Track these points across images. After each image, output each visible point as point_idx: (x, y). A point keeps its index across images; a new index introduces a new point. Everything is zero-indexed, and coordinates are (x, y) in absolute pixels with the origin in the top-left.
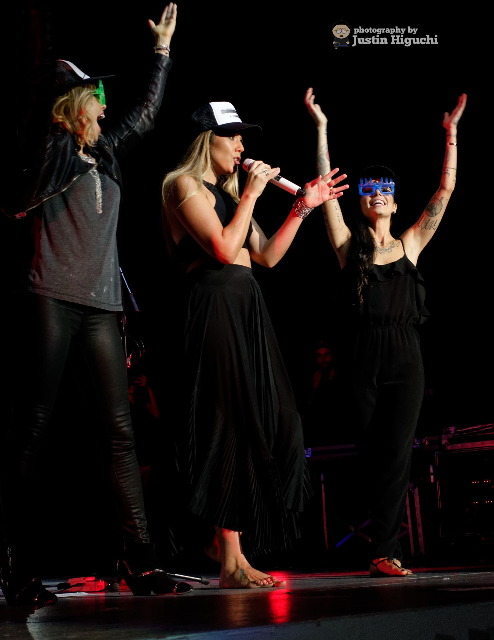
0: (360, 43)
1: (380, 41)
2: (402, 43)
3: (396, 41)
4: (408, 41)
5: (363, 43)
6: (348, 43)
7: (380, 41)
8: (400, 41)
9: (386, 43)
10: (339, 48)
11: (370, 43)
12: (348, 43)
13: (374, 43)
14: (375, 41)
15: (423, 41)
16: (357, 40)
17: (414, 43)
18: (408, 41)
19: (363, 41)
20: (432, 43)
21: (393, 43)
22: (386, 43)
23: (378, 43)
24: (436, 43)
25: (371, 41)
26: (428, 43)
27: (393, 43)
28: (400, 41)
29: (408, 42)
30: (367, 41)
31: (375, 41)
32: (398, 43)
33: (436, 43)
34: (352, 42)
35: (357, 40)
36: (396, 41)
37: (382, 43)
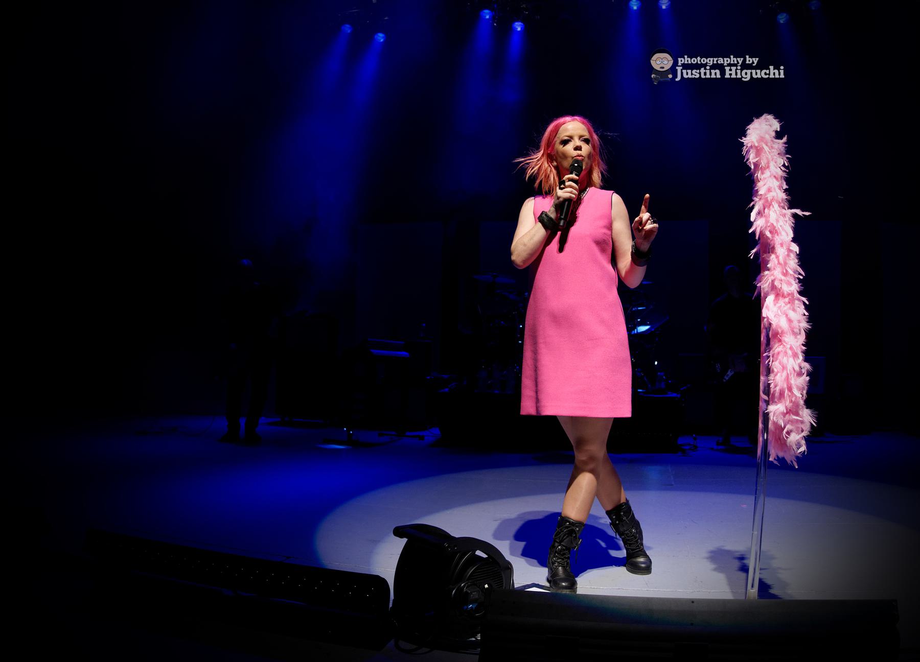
0: (685, 76)
1: (711, 74)
2: (739, 76)
3: (731, 74)
5: (690, 76)
6: (670, 76)
7: (711, 74)
8: (736, 74)
9: (719, 76)
10: (659, 83)
11: (698, 76)
12: (670, 76)
13: (703, 76)
14: (705, 74)
15: (766, 74)
16: (682, 73)
17: (754, 76)
19: (689, 74)
20: (777, 76)
21: (727, 76)
22: (719, 76)
23: (708, 76)
24: (782, 76)
26: (772, 76)
27: (727, 76)
28: (736, 74)
29: (746, 75)
30: (695, 74)
31: (705, 74)
32: (734, 76)
33: (782, 76)
34: (675, 76)
35: (682, 73)
36: (731, 74)
37: (713, 76)
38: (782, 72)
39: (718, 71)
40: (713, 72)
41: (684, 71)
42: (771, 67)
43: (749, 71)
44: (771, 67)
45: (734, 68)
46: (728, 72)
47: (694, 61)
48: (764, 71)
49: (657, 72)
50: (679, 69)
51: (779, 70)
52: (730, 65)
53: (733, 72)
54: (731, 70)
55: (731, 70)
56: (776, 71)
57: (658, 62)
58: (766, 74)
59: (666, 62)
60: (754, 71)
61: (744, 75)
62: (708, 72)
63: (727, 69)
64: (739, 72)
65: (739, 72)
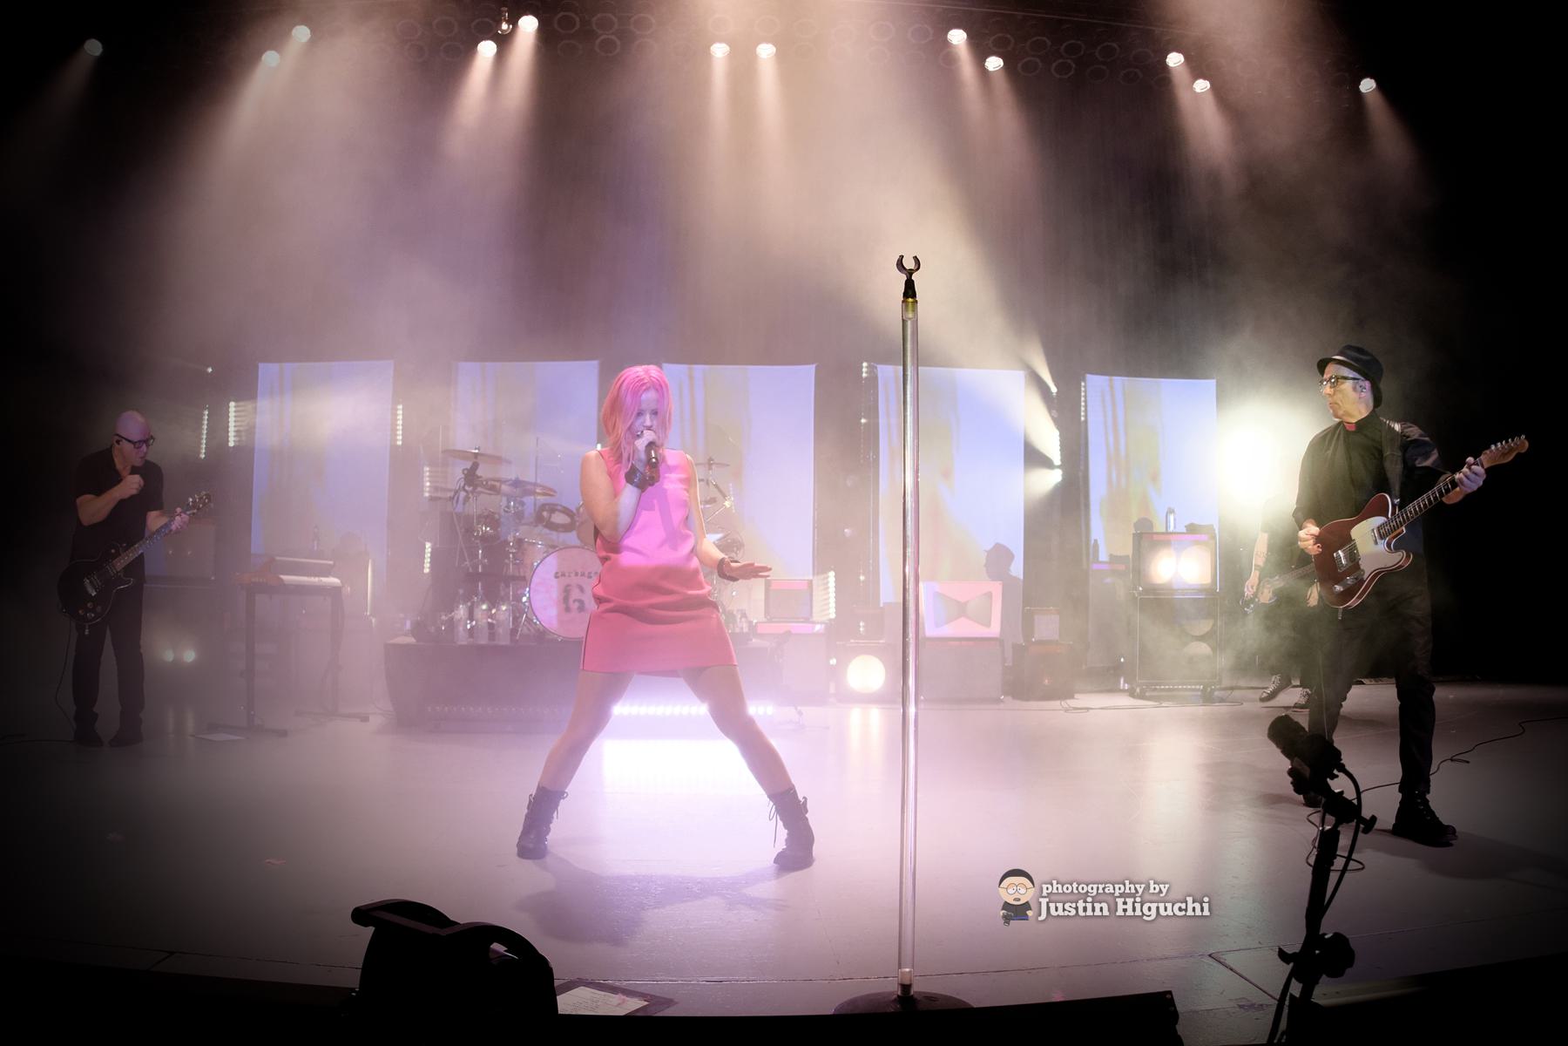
0: (1053, 912)
2: (1138, 913)
5: (1060, 912)
13: (1081, 913)
14: (1085, 909)
20: (1198, 913)
21: (1120, 913)
22: (1106, 913)
23: (1089, 913)
24: (1206, 913)
26: (1190, 913)
31: (1085, 909)
32: (1130, 912)
33: (1206, 913)
37: (1097, 913)
38: (1206, 906)
39: (1105, 906)
40: (1097, 906)
41: (1052, 906)
42: (1190, 900)
43: (1154, 906)
44: (1190, 900)
45: (1129, 901)
46: (1121, 907)
47: (1067, 889)
48: (1177, 906)
49: (1007, 906)
50: (1044, 901)
51: (1201, 903)
52: (1121, 895)
53: (1129, 907)
56: (1197, 906)
59: (1023, 891)
60: (1162, 906)
62: (1089, 906)
63: (1120, 901)
64: (1138, 906)
65: (1138, 906)
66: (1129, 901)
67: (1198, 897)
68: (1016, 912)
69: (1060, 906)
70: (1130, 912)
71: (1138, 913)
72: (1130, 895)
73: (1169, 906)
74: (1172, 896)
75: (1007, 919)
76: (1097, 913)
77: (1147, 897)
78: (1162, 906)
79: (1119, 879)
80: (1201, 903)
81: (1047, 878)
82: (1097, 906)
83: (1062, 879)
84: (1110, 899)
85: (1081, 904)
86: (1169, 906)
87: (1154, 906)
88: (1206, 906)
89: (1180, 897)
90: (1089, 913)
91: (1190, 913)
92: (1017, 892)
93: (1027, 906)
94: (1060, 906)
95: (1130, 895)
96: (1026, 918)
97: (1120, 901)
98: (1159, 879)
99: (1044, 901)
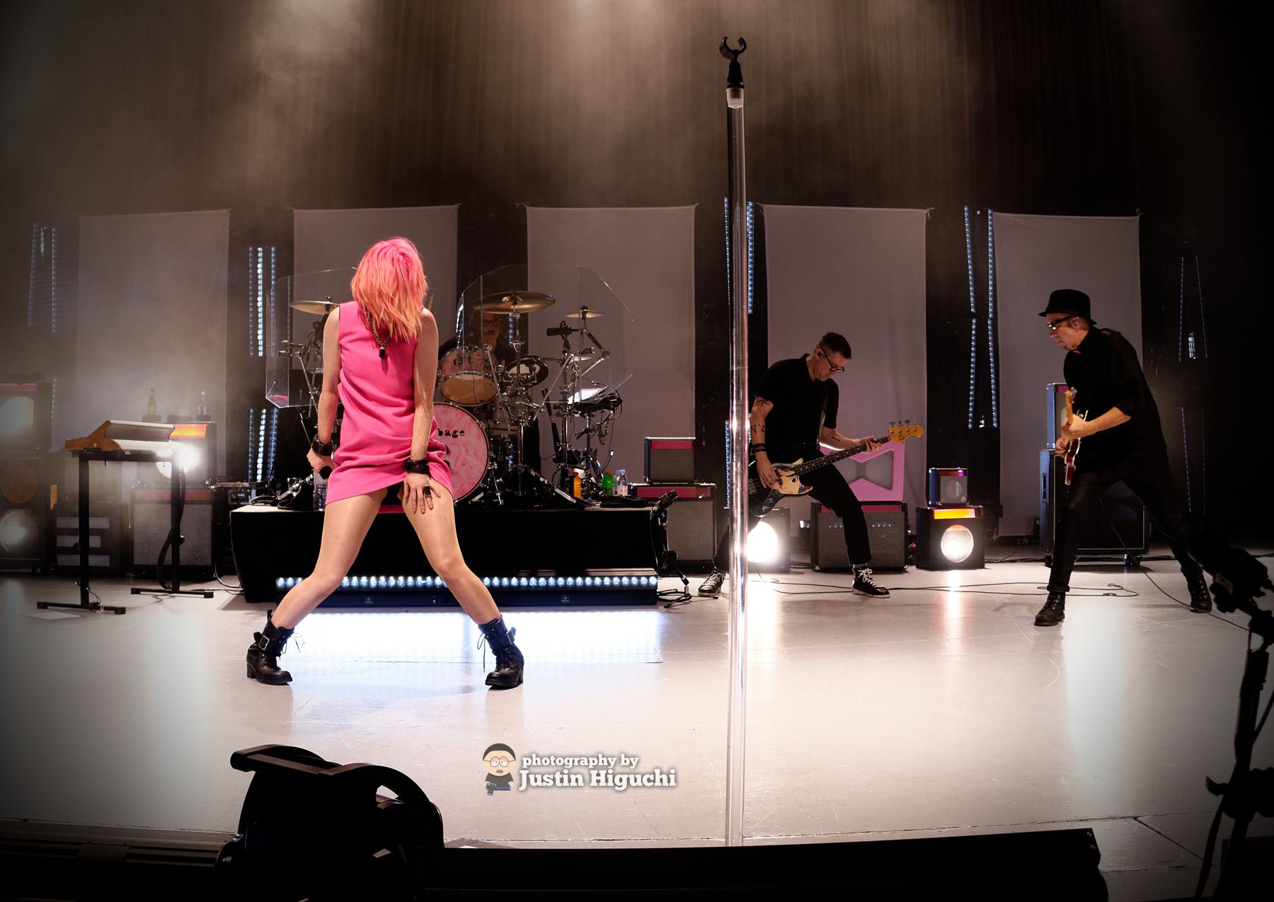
0: (532, 783)
1: (569, 781)
3: (598, 781)
4: (621, 780)
5: (539, 783)
7: (569, 781)
8: (607, 781)
13: (558, 783)
14: (562, 780)
15: (649, 780)
16: (528, 779)
18: (621, 780)
22: (580, 783)
25: (554, 780)
28: (607, 781)
31: (562, 780)
35: (528, 779)
36: (598, 781)
39: (580, 777)
41: (532, 777)
42: (658, 772)
44: (658, 772)
46: (594, 778)
49: (490, 777)
51: (668, 774)
53: (602, 778)
54: (598, 775)
55: (598, 775)
56: (665, 778)
57: (494, 764)
58: (649, 780)
59: (505, 764)
61: (617, 782)
62: (566, 778)
64: (610, 777)
65: (610, 777)
66: (603, 773)
67: (665, 770)
68: (498, 783)
69: (539, 777)
70: (603, 783)
71: (610, 783)
72: (603, 768)
73: (639, 777)
74: (642, 768)
75: (490, 790)
76: (573, 783)
77: (618, 769)
78: (632, 777)
79: (593, 752)
80: (668, 774)
81: (527, 753)
82: (573, 777)
83: (541, 753)
84: (585, 771)
85: (558, 776)
86: (639, 777)
87: (624, 777)
88: (672, 777)
89: (649, 769)
90: (566, 783)
91: (658, 783)
92: (500, 764)
93: (508, 777)
94: (539, 777)
95: (603, 768)
96: (508, 788)
97: (594, 773)
98: (630, 752)
99: (524, 773)
